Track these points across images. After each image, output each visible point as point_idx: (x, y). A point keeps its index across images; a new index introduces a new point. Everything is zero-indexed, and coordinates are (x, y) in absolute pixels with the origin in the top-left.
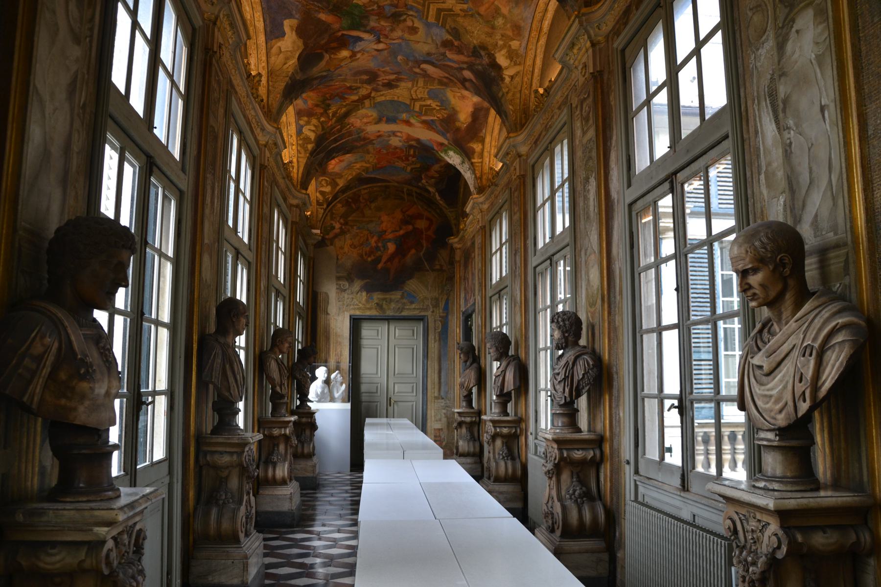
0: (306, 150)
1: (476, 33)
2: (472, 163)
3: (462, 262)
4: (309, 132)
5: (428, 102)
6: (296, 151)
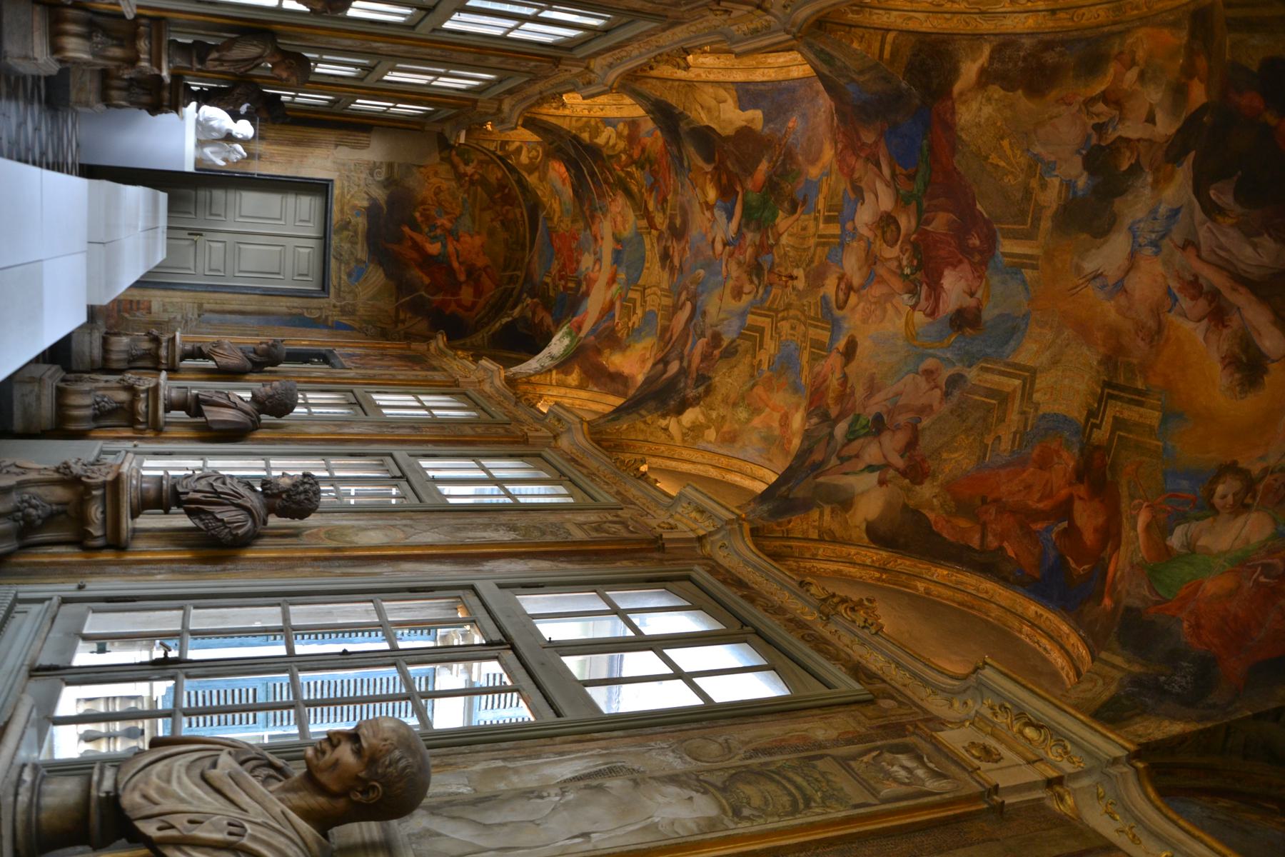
0: (582, 129)
1: (728, 380)
2: (550, 371)
3: (408, 353)
4: (606, 137)
5: (639, 311)
6: (581, 114)
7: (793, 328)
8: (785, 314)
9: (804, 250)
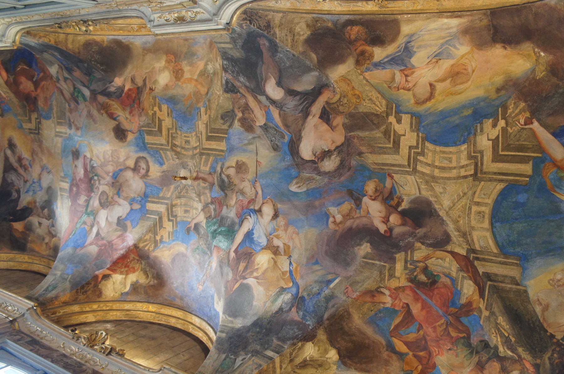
5: (484, 142)
7: (187, 142)
8: (195, 152)
9: (184, 197)
